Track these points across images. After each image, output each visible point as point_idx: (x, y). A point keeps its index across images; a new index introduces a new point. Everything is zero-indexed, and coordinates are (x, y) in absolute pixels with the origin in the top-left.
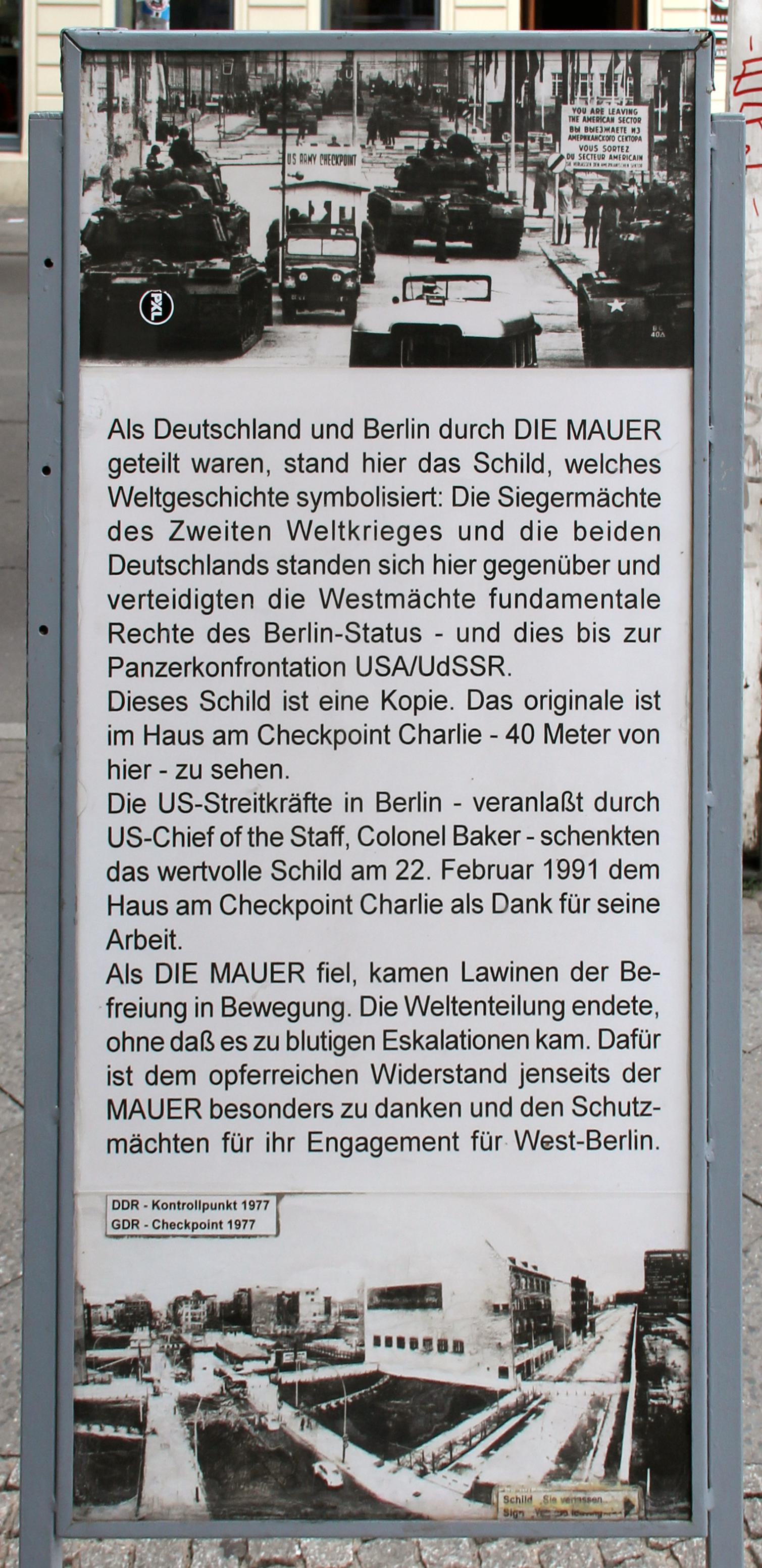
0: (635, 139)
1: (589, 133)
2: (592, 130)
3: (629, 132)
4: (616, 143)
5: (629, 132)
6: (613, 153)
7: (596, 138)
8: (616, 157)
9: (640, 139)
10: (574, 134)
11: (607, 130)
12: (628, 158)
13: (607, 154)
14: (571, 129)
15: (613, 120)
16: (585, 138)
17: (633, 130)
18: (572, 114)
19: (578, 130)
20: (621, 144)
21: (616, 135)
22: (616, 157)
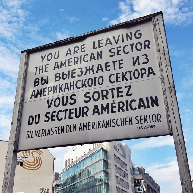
0: (141, 73)
1: (62, 82)
2: (66, 76)
3: (128, 66)
4: (107, 85)
5: (128, 66)
6: (99, 103)
7: (73, 85)
8: (105, 109)
9: (151, 71)
10: (40, 87)
11: (90, 70)
12: (129, 106)
13: (91, 105)
14: (36, 82)
15: (100, 55)
16: (55, 89)
17: (136, 61)
18: (40, 64)
19: (46, 81)
20: (116, 85)
21: (106, 75)
22: (105, 109)
